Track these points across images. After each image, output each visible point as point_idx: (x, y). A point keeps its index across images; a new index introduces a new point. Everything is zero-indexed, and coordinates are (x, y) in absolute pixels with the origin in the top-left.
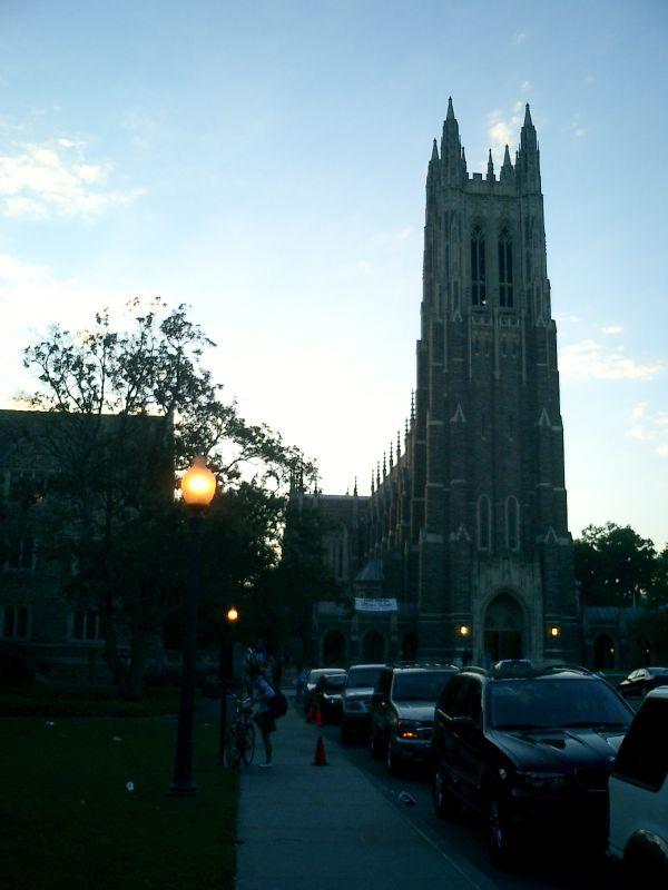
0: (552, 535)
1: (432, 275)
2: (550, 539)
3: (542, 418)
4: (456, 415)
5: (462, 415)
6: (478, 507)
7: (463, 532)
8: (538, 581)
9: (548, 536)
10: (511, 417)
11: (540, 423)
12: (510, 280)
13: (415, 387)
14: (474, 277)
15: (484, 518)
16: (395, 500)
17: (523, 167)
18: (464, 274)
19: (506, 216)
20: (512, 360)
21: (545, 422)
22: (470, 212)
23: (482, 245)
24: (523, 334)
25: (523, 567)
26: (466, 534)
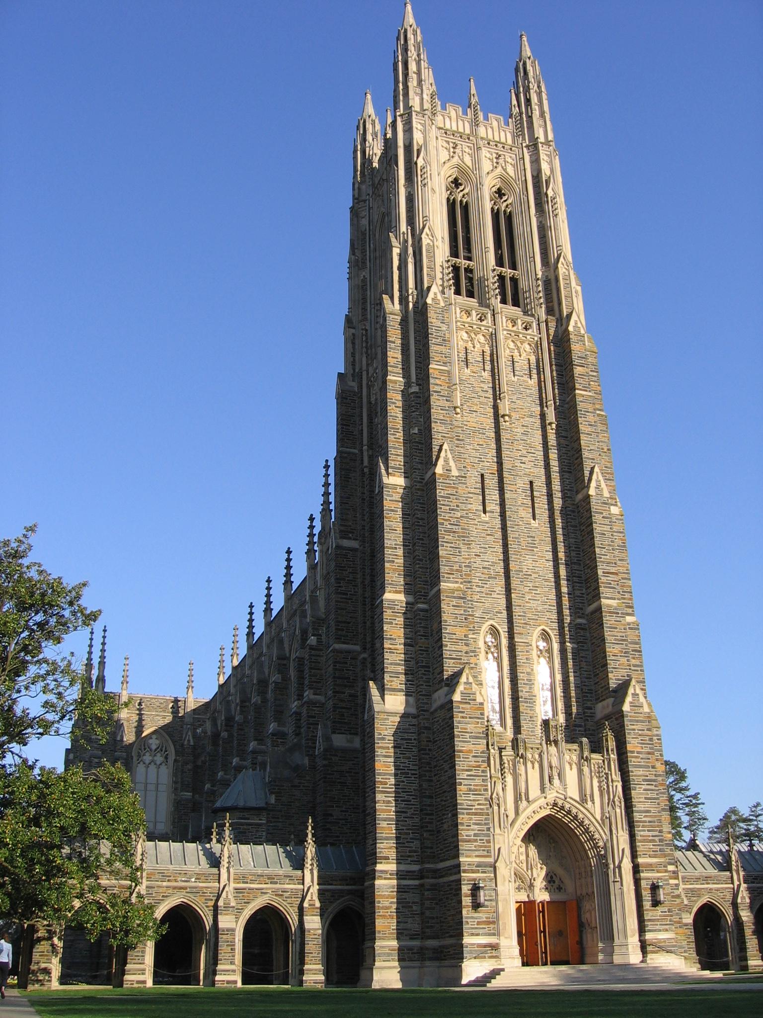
1: (365, 273)
3: (593, 484)
5: (452, 463)
10: (531, 483)
13: (330, 451)
14: (454, 253)
16: (282, 668)
21: (598, 487)
23: (465, 208)
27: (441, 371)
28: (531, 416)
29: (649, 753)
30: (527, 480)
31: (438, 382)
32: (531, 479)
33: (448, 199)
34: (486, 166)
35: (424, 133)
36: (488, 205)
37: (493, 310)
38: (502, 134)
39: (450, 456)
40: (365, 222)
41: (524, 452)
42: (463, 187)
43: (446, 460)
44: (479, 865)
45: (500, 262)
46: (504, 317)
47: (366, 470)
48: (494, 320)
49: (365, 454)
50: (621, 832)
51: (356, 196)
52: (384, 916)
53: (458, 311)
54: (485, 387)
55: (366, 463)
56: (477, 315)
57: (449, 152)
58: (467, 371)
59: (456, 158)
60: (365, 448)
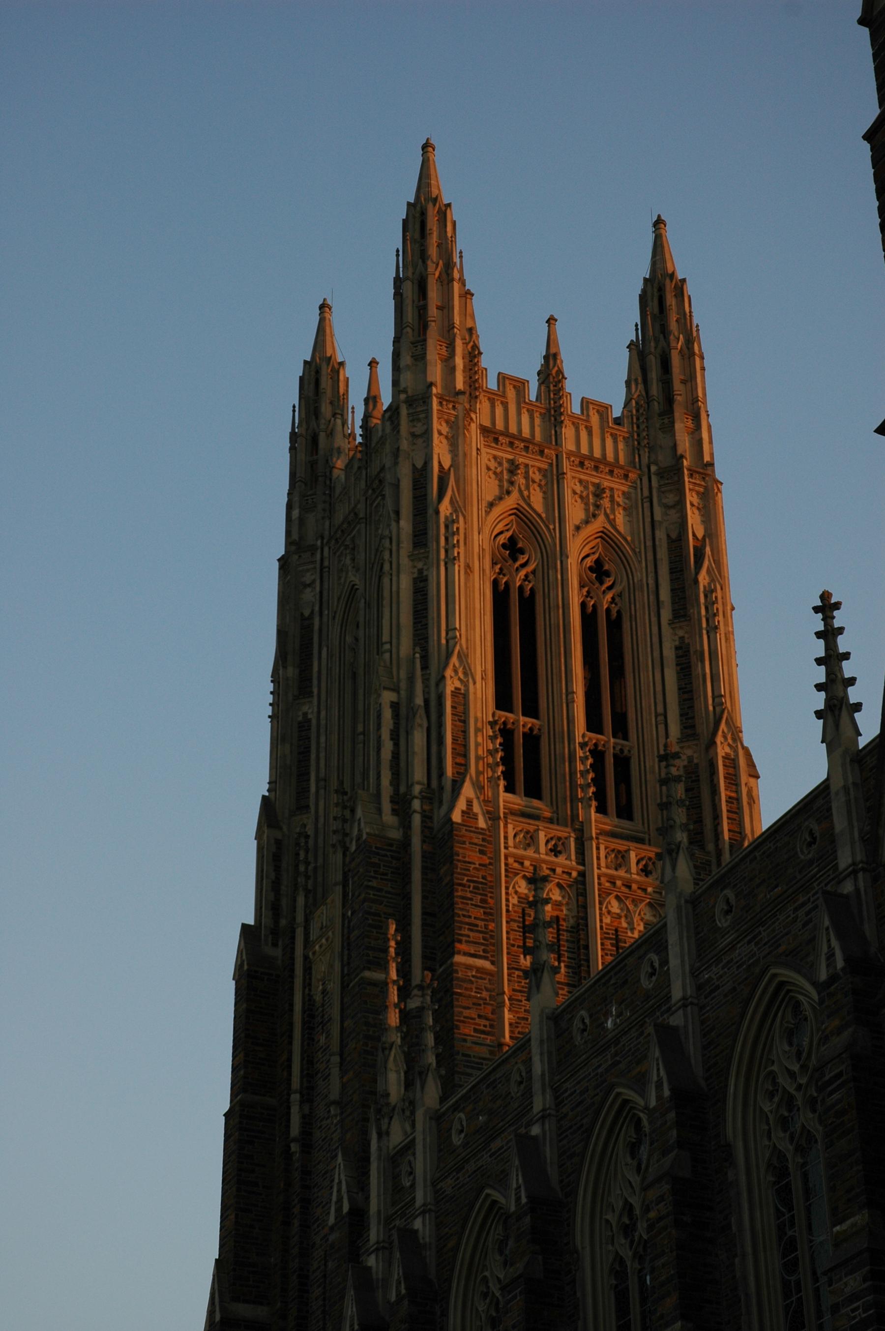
1: (309, 709)
14: (503, 701)
17: (655, 390)
33: (495, 583)
34: (575, 512)
35: (454, 442)
37: (581, 831)
38: (609, 442)
40: (309, 596)
42: (526, 557)
45: (594, 724)
47: (294, 1147)
48: (583, 854)
49: (295, 1110)
51: (295, 536)
55: (295, 1129)
56: (547, 842)
57: (501, 480)
59: (515, 494)
60: (295, 1097)
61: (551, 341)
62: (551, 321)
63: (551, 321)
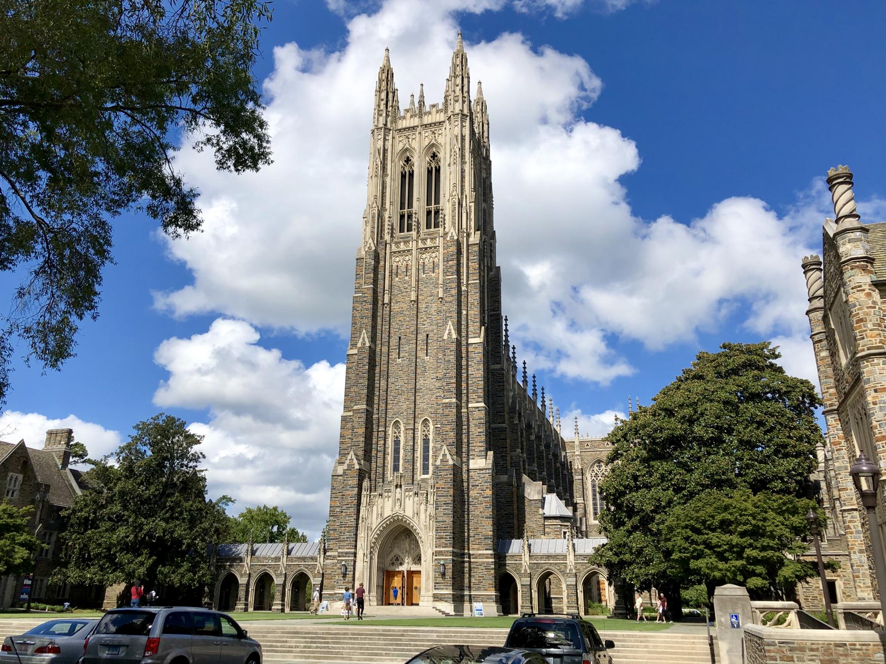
0: (444, 455)
2: (442, 461)
4: (361, 340)
5: (367, 340)
6: (390, 431)
7: (351, 459)
8: (431, 509)
9: (441, 457)
10: (427, 335)
11: (445, 337)
12: (437, 201)
15: (397, 443)
18: (387, 206)
19: (433, 141)
20: (431, 279)
21: (449, 333)
22: (399, 147)
23: (411, 175)
24: (441, 249)
25: (416, 494)
26: (355, 461)
27: (367, 289)
28: (431, 296)
29: (449, 488)
30: (425, 334)
31: (366, 295)
32: (428, 333)
36: (425, 166)
39: (366, 336)
41: (425, 318)
43: (364, 339)
44: (346, 553)
46: (420, 241)
50: (431, 534)
52: (328, 579)
53: (393, 245)
54: (406, 286)
58: (397, 279)
61: (422, 91)
62: (422, 85)
63: (422, 85)
